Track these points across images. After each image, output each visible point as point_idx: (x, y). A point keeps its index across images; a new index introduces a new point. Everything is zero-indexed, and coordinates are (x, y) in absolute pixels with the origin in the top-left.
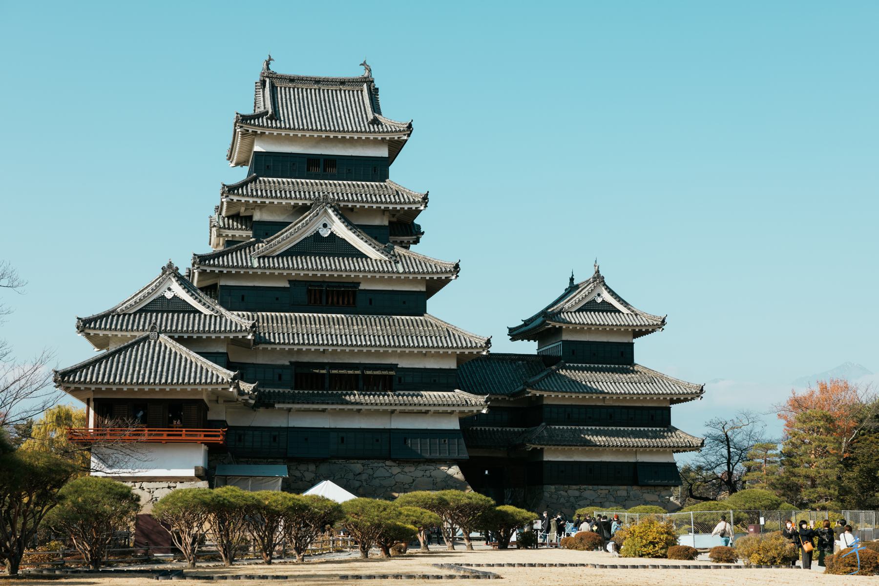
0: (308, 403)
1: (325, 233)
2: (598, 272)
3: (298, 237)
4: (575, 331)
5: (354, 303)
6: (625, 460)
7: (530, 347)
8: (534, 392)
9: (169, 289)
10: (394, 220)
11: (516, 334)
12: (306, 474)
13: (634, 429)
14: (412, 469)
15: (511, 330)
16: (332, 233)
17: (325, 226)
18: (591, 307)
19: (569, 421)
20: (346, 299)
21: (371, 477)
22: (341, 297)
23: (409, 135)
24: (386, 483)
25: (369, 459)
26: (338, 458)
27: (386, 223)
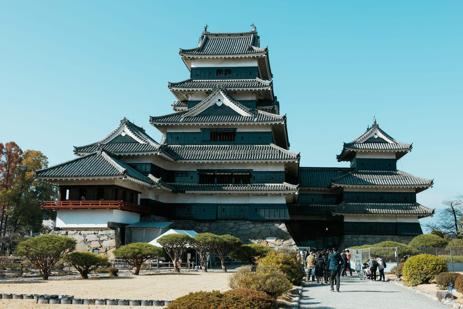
0: (202, 190)
1: (219, 104)
2: (375, 122)
3: (206, 106)
4: (361, 153)
5: (234, 139)
6: (391, 221)
7: (347, 164)
8: (336, 185)
9: (124, 131)
10: (262, 98)
11: (340, 158)
12: (204, 228)
13: (395, 204)
14: (260, 225)
15: (337, 156)
16: (223, 104)
17: (219, 100)
18: (372, 140)
19: (358, 200)
20: (230, 137)
21: (238, 230)
22: (226, 136)
23: (267, 54)
24: (245, 233)
25: (237, 220)
26: (221, 220)
27: (254, 98)
